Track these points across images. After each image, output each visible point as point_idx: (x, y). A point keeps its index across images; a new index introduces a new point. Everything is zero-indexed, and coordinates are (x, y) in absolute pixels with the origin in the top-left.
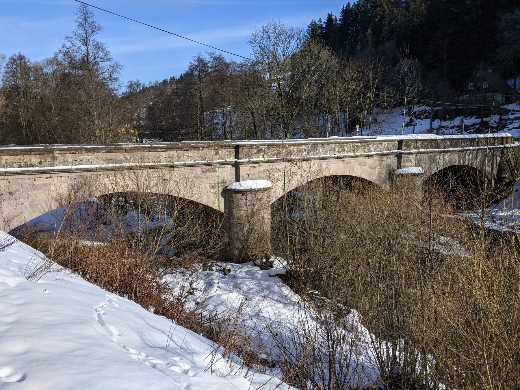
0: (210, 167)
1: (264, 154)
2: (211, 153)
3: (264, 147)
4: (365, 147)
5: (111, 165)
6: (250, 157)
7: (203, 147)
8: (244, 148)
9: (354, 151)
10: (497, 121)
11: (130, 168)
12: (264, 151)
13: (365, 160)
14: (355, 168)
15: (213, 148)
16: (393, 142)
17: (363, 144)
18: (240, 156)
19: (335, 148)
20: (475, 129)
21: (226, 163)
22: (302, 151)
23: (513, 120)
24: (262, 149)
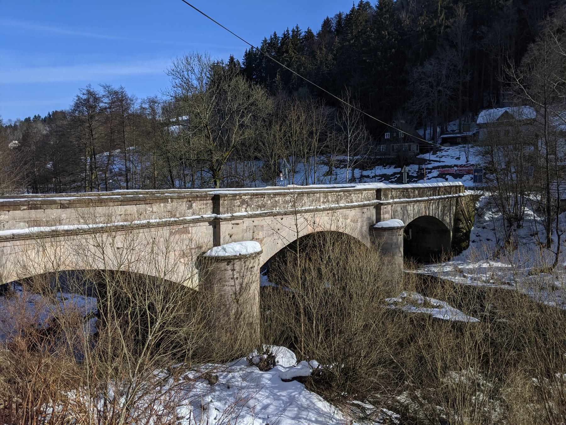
0: (181, 227)
1: (247, 207)
2: (183, 206)
3: (247, 197)
4: (347, 197)
5: (35, 229)
6: (232, 211)
7: (172, 198)
8: (226, 198)
10: (417, 170)
11: (68, 233)
12: (247, 203)
13: (347, 212)
15: (185, 200)
16: (372, 192)
18: (221, 209)
19: (320, 197)
20: (396, 179)
21: (202, 220)
23: (431, 169)
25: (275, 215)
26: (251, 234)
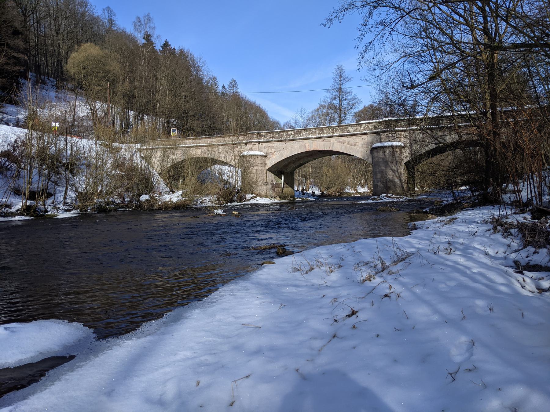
4: (343, 129)
9: (333, 133)
12: (264, 136)
13: (345, 139)
14: (335, 145)
19: (315, 131)
22: (289, 135)
25: (280, 141)
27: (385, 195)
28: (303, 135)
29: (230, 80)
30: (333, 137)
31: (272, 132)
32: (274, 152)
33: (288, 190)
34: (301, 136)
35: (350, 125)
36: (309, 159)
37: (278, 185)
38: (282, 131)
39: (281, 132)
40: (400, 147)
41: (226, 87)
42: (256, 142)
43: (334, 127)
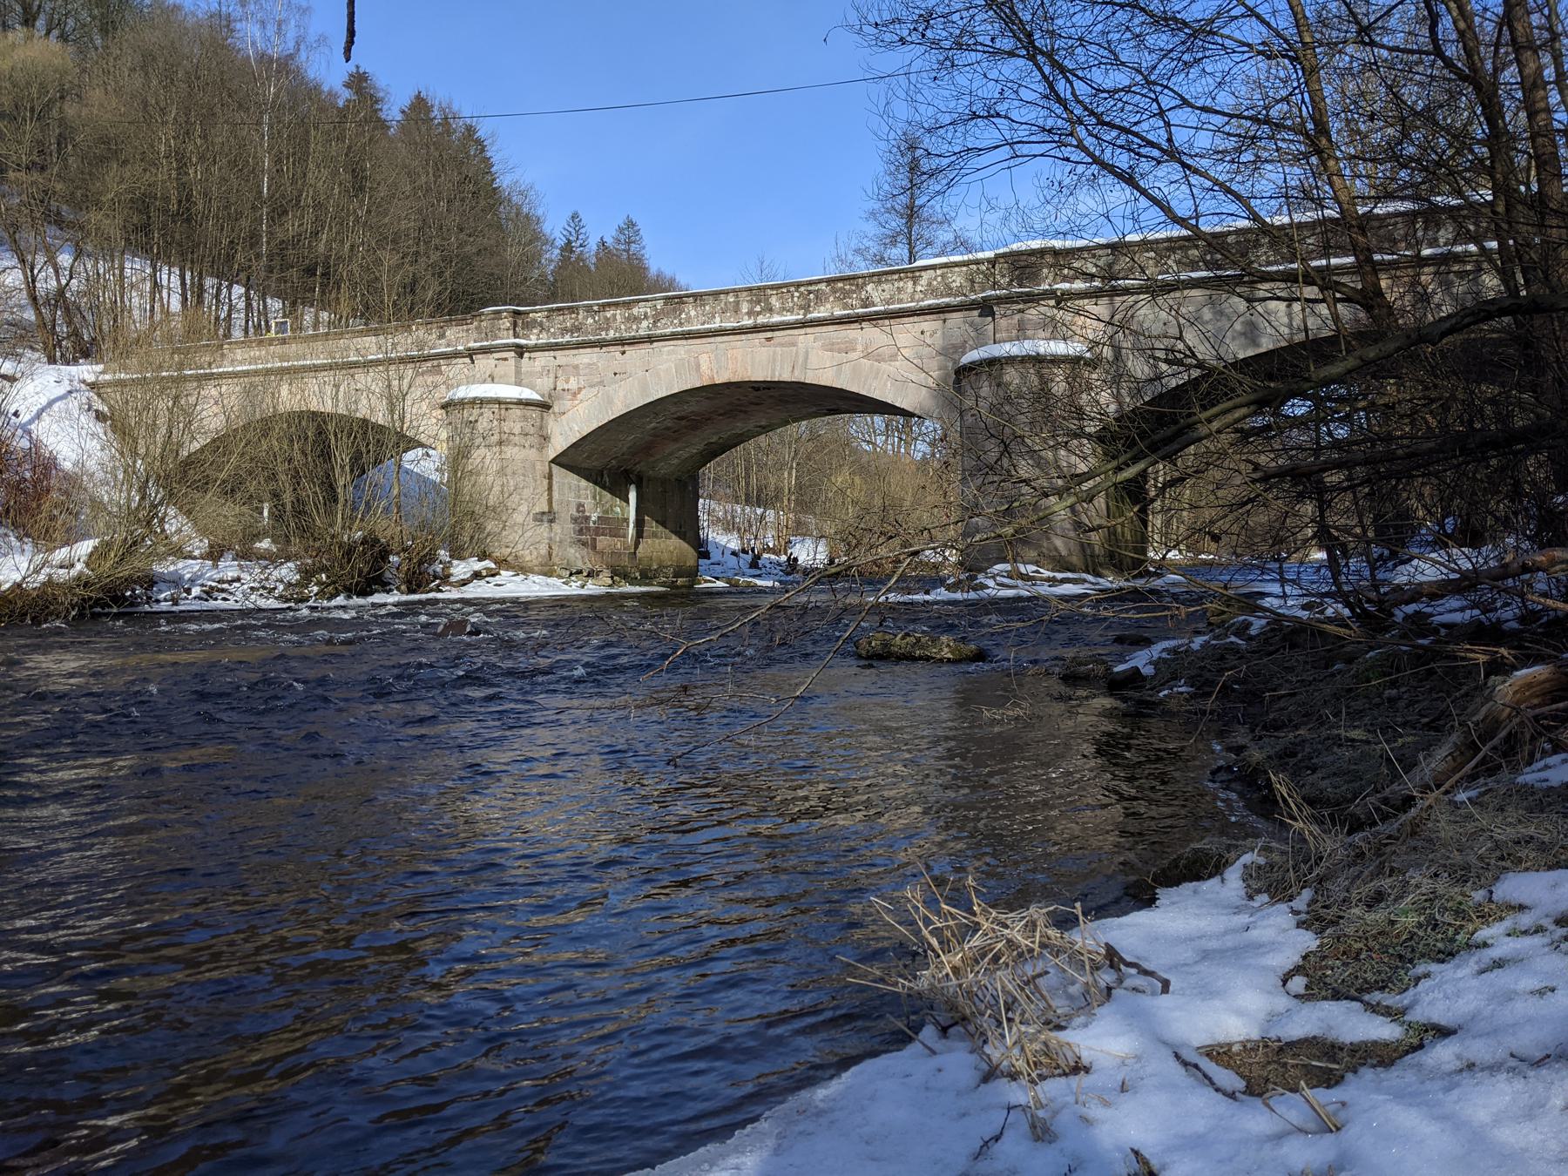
4: (847, 294)
12: (541, 324)
13: (851, 333)
17: (840, 285)
19: (737, 303)
22: (637, 320)
24: (535, 321)
25: (601, 344)
26: (552, 380)
27: (1007, 567)
28: (689, 320)
29: (621, 221)
30: (803, 324)
31: (572, 310)
32: (580, 389)
33: (665, 546)
34: (681, 324)
35: (873, 275)
36: (740, 426)
37: (612, 526)
38: (609, 305)
39: (604, 307)
40: (1075, 361)
41: (609, 241)
42: (506, 348)
43: (810, 283)
